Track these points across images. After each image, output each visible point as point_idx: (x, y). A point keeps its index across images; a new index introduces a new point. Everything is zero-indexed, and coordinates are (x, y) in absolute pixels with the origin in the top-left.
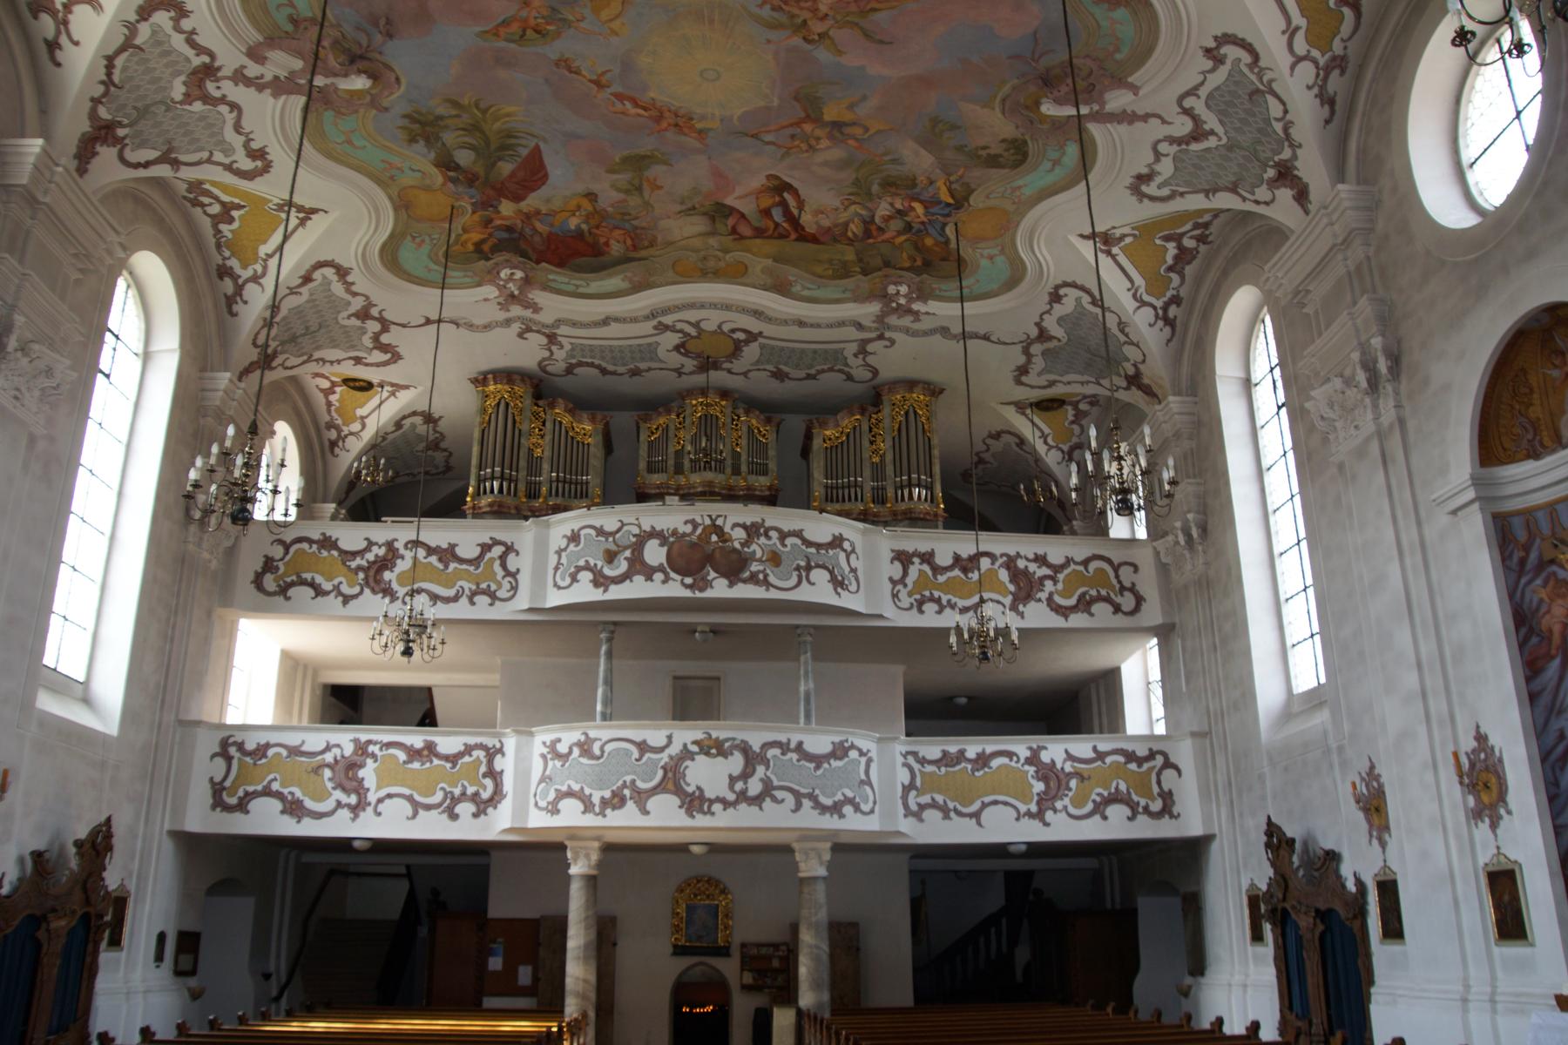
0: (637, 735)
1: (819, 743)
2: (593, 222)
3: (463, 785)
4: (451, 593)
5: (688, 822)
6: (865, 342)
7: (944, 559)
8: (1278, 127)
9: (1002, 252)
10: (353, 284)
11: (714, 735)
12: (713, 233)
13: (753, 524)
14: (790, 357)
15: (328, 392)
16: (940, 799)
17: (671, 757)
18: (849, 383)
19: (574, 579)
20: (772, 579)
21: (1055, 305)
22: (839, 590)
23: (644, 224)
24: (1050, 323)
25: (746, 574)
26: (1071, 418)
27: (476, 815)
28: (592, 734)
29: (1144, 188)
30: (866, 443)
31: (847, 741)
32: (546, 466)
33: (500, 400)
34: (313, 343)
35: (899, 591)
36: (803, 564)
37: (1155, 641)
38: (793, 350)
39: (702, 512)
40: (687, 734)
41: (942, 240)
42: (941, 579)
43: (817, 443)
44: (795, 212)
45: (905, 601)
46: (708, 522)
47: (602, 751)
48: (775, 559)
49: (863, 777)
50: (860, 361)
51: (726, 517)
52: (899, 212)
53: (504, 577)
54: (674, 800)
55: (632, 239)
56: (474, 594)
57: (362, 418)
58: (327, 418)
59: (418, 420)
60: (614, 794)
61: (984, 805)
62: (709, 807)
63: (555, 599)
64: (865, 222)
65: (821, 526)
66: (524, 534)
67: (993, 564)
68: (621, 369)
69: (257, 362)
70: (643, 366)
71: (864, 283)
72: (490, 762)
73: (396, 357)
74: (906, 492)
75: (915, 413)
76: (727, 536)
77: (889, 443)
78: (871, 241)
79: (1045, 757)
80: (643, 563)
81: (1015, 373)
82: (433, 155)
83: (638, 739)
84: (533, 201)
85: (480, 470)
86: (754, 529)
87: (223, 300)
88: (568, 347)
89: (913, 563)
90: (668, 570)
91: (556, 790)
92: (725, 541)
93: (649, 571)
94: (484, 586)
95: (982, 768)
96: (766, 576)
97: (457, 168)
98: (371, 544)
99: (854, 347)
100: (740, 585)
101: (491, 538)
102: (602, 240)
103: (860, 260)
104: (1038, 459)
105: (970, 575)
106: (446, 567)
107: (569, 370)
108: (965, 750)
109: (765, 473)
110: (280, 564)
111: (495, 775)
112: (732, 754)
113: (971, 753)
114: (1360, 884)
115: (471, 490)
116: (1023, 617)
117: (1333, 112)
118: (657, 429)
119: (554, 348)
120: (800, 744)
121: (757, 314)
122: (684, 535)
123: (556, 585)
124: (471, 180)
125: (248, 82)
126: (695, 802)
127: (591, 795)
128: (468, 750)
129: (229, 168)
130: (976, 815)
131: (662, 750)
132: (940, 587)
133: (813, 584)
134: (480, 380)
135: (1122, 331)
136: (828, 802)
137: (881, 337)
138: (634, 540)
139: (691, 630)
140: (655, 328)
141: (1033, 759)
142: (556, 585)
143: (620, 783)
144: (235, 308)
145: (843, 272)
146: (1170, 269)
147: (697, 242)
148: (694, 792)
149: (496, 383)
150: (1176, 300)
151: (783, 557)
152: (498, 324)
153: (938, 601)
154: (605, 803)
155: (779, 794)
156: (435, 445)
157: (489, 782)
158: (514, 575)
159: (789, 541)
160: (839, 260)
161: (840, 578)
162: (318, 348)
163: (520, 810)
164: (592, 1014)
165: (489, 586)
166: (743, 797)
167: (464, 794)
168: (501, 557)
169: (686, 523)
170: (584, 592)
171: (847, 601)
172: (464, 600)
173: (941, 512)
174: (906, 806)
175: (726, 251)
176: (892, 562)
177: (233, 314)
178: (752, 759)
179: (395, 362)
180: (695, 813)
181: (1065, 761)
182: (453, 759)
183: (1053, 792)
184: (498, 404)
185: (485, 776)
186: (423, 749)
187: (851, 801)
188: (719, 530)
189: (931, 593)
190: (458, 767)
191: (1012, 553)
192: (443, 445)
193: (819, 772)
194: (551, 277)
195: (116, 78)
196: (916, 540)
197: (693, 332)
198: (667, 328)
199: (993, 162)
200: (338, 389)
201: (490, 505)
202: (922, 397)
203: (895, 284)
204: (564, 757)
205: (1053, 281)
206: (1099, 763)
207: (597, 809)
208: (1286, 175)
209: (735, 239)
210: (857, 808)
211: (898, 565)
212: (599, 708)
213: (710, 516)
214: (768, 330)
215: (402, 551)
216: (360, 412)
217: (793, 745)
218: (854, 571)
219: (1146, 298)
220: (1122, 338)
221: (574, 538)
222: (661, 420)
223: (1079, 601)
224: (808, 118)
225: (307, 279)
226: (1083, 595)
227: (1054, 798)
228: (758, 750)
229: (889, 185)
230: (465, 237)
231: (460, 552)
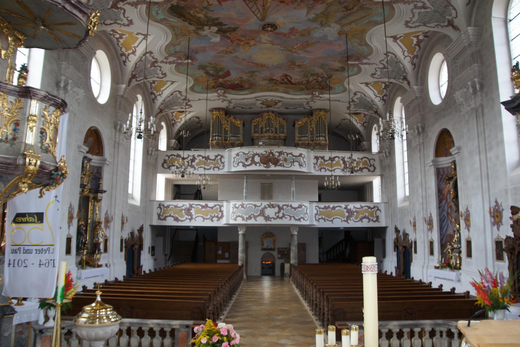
1: (295, 205)
4: (208, 167)
5: (265, 223)
7: (327, 158)
8: (403, 69)
9: (341, 86)
11: (272, 203)
16: (323, 217)
19: (238, 165)
20: (285, 165)
24: (355, 99)
27: (218, 221)
28: (244, 203)
29: (374, 76)
32: (229, 133)
36: (292, 161)
39: (268, 149)
40: (265, 203)
42: (326, 163)
43: (296, 125)
44: (290, 79)
45: (317, 168)
46: (270, 151)
47: (246, 206)
48: (286, 160)
50: (307, 105)
52: (315, 79)
57: (181, 118)
58: (172, 118)
59: (195, 118)
60: (249, 216)
61: (334, 219)
63: (234, 169)
64: (307, 81)
65: (296, 151)
66: (226, 153)
70: (253, 107)
71: (307, 92)
74: (319, 138)
77: (315, 125)
79: (349, 207)
80: (254, 161)
82: (204, 72)
83: (254, 204)
84: (227, 79)
87: (152, 100)
93: (256, 164)
94: (216, 166)
97: (210, 73)
98: (189, 156)
99: (306, 103)
104: (355, 126)
107: (234, 108)
109: (283, 133)
110: (168, 161)
111: (221, 211)
114: (412, 241)
115: (210, 139)
117: (415, 67)
120: (291, 205)
121: (281, 97)
122: (264, 154)
123: (234, 166)
124: (213, 75)
125: (164, 62)
126: (267, 218)
128: (215, 206)
129: (158, 77)
130: (332, 221)
131: (259, 206)
132: (326, 165)
136: (297, 218)
137: (312, 101)
139: (265, 175)
141: (346, 208)
142: (234, 166)
144: (155, 101)
145: (302, 90)
146: (384, 89)
150: (386, 95)
152: (217, 100)
153: (325, 169)
154: (247, 218)
155: (286, 216)
156: (199, 123)
157: (220, 213)
159: (289, 155)
163: (228, 219)
164: (244, 265)
166: (278, 217)
167: (215, 216)
170: (241, 168)
172: (212, 169)
173: (327, 143)
174: (316, 218)
175: (273, 86)
177: (154, 103)
178: (280, 208)
182: (212, 208)
183: (350, 216)
187: (302, 218)
188: (272, 153)
191: (344, 156)
192: (200, 122)
195: (137, 67)
196: (320, 154)
197: (265, 101)
198: (259, 100)
199: (337, 70)
201: (216, 143)
203: (315, 92)
205: (354, 92)
208: (405, 78)
210: (304, 219)
211: (315, 160)
212: (244, 194)
214: (284, 100)
215: (196, 157)
216: (180, 117)
217: (289, 205)
218: (304, 162)
219: (378, 95)
220: (373, 103)
221: (238, 155)
222: (257, 119)
224: (292, 64)
225: (172, 94)
227: (351, 217)
229: (312, 75)
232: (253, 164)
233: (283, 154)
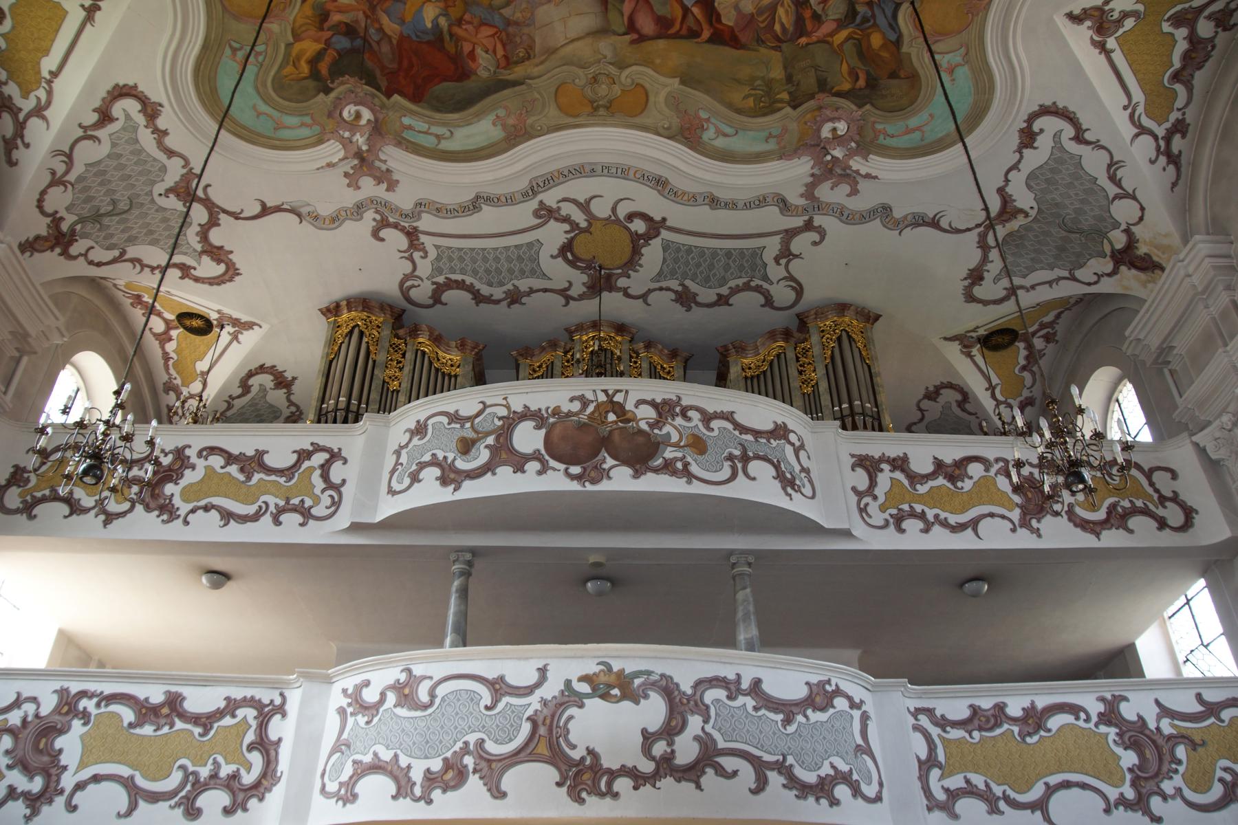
0: (490, 670)
2: (455, 13)
3: (215, 762)
4: (251, 510)
6: (790, 234)
10: (165, 133)
11: (616, 666)
12: (603, 31)
13: (665, 402)
14: (698, 265)
15: (164, 338)
16: (978, 780)
17: (545, 703)
18: (767, 309)
19: (415, 478)
20: (694, 469)
21: (1026, 152)
22: (789, 490)
23: (518, 15)
25: (659, 462)
26: (1022, 362)
27: (228, 811)
28: (418, 670)
30: (793, 372)
31: (829, 682)
33: (353, 328)
34: (123, 231)
35: (867, 505)
37: (1202, 582)
38: (702, 251)
39: (595, 388)
41: (893, 37)
42: (922, 489)
45: (878, 518)
46: (602, 398)
47: (432, 695)
48: (698, 445)
49: (860, 741)
51: (627, 392)
53: (323, 491)
54: (550, 773)
55: (504, 45)
56: (281, 511)
58: (165, 378)
59: (267, 380)
60: (448, 765)
61: (1051, 790)
62: (609, 784)
63: (388, 508)
67: (987, 470)
68: (498, 293)
69: (45, 239)
70: (523, 285)
72: (263, 726)
73: (231, 272)
75: (849, 337)
76: (629, 416)
77: (821, 371)
78: (803, 40)
79: (1128, 711)
80: (512, 451)
81: (966, 283)
83: (491, 675)
85: (323, 402)
86: (667, 408)
88: (433, 254)
89: (882, 470)
90: (547, 457)
91: (355, 762)
92: (629, 421)
93: (519, 463)
94: (296, 501)
95: (1036, 732)
96: (686, 465)
100: (650, 475)
101: (312, 444)
102: (467, 48)
103: (789, 79)
105: (959, 484)
106: (249, 478)
107: (436, 298)
108: (1005, 705)
111: (266, 747)
112: (646, 697)
113: (1015, 708)
116: (1039, 536)
118: (540, 367)
119: (417, 255)
120: (757, 683)
122: (569, 414)
127: (409, 767)
128: (232, 706)
130: (1040, 806)
131: (529, 690)
132: (921, 499)
133: (754, 479)
134: (332, 311)
135: (1113, 178)
136: (810, 778)
137: (808, 226)
138: (500, 423)
140: (536, 214)
141: (1110, 715)
143: (460, 745)
144: (16, 154)
147: (584, 49)
148: (583, 759)
149: (349, 310)
150: (1180, 128)
151: (709, 443)
153: (922, 516)
154: (431, 779)
155: (729, 763)
157: (256, 758)
158: (337, 488)
159: (715, 424)
160: (763, 78)
161: (789, 476)
162: (132, 240)
165: (302, 501)
166: (666, 766)
167: (214, 776)
168: (322, 466)
169: (572, 400)
171: (798, 505)
172: (267, 519)
175: (622, 66)
176: (853, 470)
177: (12, 163)
179: (231, 280)
180: (584, 795)
181: (1159, 718)
182: (205, 721)
183: (1153, 768)
184: (351, 332)
185: (251, 748)
186: (162, 705)
187: (846, 778)
188: (619, 409)
189: (911, 507)
190: (212, 732)
193: (791, 729)
194: (406, 121)
197: (579, 218)
200: (174, 333)
202: (855, 322)
203: (832, 120)
204: (369, 709)
206: (1212, 720)
207: (418, 791)
209: (633, 42)
210: (857, 792)
213: (605, 391)
215: (194, 459)
216: (202, 366)
217: (745, 685)
218: (806, 471)
220: (1112, 190)
221: (420, 430)
223: (1109, 513)
225: (105, 117)
226: (1113, 507)
227: (1158, 776)
228: (689, 692)
230: (298, 47)
231: (269, 460)
232: (504, 463)
233: (684, 414)
